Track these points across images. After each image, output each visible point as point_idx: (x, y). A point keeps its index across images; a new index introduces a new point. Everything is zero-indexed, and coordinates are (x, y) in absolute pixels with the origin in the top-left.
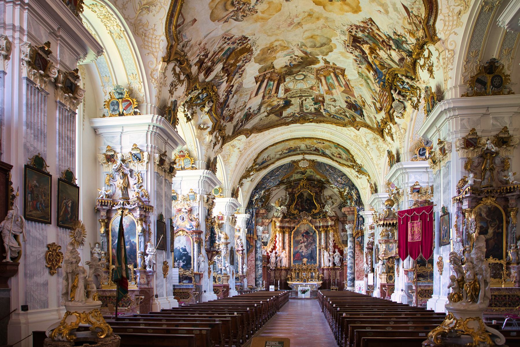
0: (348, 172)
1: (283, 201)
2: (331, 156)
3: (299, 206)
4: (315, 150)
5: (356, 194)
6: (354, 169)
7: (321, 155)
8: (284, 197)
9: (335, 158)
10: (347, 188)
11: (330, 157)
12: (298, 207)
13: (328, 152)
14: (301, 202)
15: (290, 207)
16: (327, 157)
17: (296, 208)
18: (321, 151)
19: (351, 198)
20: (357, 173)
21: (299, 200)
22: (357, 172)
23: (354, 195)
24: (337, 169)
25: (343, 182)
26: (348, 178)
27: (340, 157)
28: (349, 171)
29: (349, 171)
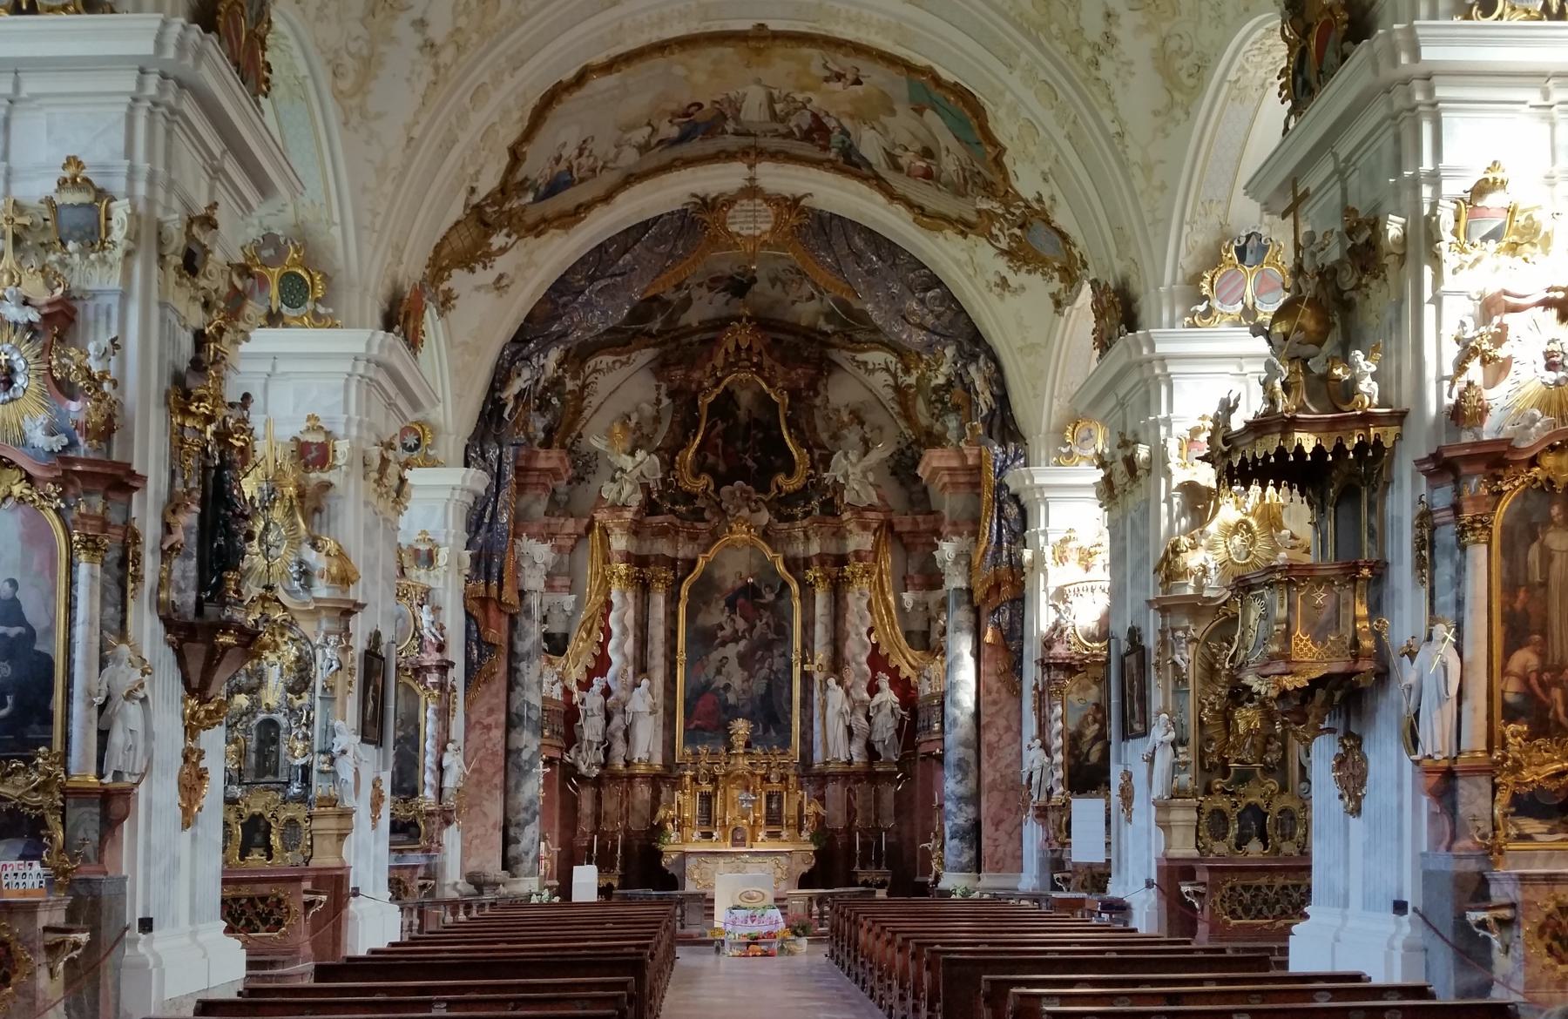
0: (957, 262)
1: (646, 430)
2: (883, 169)
3: (716, 455)
4: (807, 136)
5: (988, 381)
6: (992, 238)
7: (835, 167)
8: (648, 410)
9: (899, 183)
10: (950, 352)
11: (877, 177)
12: (711, 459)
13: (870, 146)
14: (725, 435)
15: (673, 461)
16: (864, 179)
17: (700, 468)
18: (836, 137)
19: (966, 406)
20: (1002, 264)
21: (714, 425)
22: (1003, 252)
23: (979, 384)
24: (904, 251)
25: (930, 320)
26: (954, 300)
27: (928, 175)
28: (964, 257)
29: (964, 257)
